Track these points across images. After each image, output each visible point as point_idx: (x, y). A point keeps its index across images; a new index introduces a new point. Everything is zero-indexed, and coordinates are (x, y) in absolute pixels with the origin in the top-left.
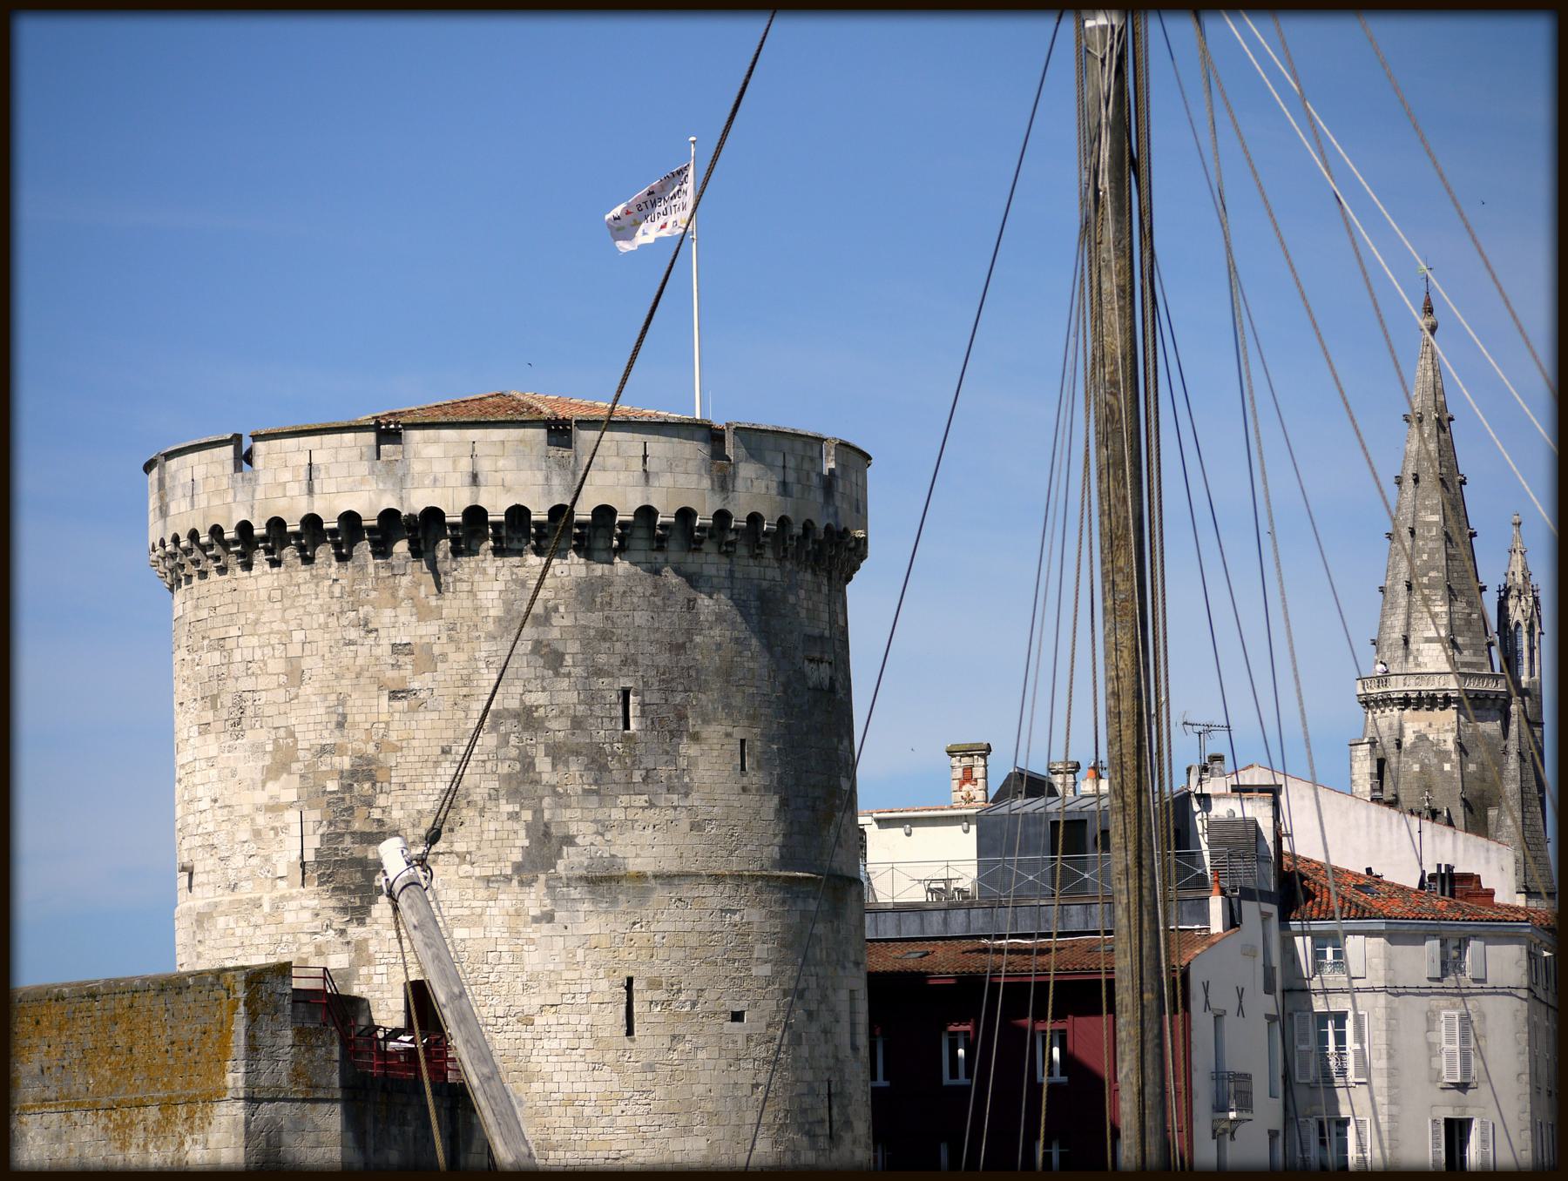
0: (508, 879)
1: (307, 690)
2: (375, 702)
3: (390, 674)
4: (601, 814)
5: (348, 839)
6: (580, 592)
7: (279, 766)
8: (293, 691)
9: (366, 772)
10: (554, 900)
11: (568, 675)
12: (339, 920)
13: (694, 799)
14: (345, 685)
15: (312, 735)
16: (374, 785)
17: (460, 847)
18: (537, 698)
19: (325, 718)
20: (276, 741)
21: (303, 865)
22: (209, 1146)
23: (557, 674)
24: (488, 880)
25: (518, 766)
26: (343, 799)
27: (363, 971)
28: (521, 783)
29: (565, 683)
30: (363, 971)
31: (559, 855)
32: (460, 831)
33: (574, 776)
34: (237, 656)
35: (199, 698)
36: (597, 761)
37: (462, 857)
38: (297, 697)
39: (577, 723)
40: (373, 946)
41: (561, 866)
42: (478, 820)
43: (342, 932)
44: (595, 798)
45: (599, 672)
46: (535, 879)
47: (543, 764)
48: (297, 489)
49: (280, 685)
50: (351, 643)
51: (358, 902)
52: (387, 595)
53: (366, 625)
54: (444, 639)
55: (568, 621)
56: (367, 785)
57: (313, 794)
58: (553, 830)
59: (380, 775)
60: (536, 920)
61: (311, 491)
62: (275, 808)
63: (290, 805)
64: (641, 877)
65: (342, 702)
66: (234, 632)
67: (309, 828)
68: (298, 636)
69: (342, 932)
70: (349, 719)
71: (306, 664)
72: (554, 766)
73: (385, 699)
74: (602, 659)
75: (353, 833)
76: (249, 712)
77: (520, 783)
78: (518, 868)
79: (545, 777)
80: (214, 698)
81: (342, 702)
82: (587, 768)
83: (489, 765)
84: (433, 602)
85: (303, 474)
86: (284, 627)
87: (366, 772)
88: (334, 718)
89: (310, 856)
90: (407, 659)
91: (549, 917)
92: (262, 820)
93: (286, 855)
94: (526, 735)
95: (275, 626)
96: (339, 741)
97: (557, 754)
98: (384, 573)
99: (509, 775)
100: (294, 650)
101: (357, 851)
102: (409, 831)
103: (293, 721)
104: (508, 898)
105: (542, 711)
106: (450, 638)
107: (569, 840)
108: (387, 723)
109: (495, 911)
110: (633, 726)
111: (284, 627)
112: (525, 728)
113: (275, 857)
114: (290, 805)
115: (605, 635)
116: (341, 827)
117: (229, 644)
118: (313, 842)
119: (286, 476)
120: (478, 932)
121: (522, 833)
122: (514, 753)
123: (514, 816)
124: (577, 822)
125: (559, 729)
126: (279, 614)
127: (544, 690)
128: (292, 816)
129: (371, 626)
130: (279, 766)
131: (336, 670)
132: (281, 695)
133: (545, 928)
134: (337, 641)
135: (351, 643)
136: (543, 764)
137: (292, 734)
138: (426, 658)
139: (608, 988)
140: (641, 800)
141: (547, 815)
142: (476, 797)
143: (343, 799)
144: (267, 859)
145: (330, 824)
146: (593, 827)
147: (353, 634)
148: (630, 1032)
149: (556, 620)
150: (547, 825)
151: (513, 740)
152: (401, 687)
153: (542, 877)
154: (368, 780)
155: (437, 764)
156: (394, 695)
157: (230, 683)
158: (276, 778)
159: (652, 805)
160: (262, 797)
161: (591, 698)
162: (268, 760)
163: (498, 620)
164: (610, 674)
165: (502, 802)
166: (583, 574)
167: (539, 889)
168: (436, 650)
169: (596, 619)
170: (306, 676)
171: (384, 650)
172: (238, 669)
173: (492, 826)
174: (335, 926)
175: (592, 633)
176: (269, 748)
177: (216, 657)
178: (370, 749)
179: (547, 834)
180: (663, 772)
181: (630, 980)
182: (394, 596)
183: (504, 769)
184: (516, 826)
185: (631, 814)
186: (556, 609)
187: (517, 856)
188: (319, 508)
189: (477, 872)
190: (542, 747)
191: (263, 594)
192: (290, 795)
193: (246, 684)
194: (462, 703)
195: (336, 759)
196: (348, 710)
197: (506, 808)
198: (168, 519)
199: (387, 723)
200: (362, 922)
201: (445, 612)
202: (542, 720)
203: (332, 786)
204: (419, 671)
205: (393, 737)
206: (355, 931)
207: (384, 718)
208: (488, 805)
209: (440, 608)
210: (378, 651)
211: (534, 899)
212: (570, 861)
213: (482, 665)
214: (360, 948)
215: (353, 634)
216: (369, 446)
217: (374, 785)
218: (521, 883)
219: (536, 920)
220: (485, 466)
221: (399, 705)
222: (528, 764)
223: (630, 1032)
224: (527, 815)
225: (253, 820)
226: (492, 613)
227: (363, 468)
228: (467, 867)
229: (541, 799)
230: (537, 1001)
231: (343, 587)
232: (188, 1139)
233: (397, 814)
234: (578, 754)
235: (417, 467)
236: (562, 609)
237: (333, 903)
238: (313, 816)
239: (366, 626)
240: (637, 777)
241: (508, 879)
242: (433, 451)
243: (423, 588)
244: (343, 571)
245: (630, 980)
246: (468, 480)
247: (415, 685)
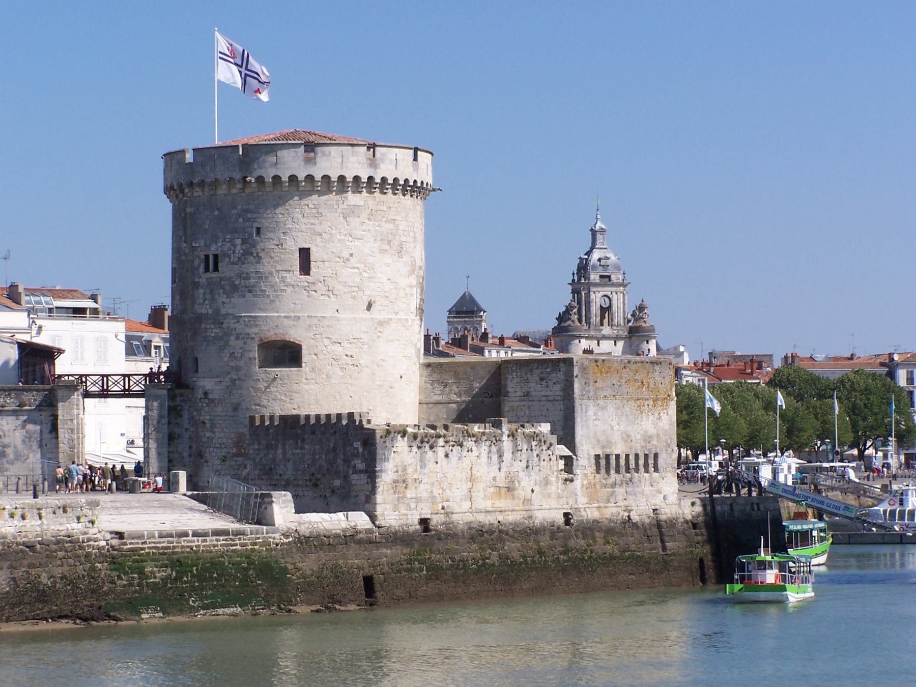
7: (412, 272)
22: (669, 414)
35: (379, 239)
63: (414, 286)
66: (399, 218)
76: (404, 249)
80: (389, 242)
89: (418, 306)
117: (397, 222)
128: (415, 289)
137: (415, 261)
157: (397, 237)
172: (400, 232)
176: (410, 264)
177: (391, 226)
192: (414, 283)
193: (403, 238)
198: (378, 171)
232: (662, 413)
238: (419, 290)
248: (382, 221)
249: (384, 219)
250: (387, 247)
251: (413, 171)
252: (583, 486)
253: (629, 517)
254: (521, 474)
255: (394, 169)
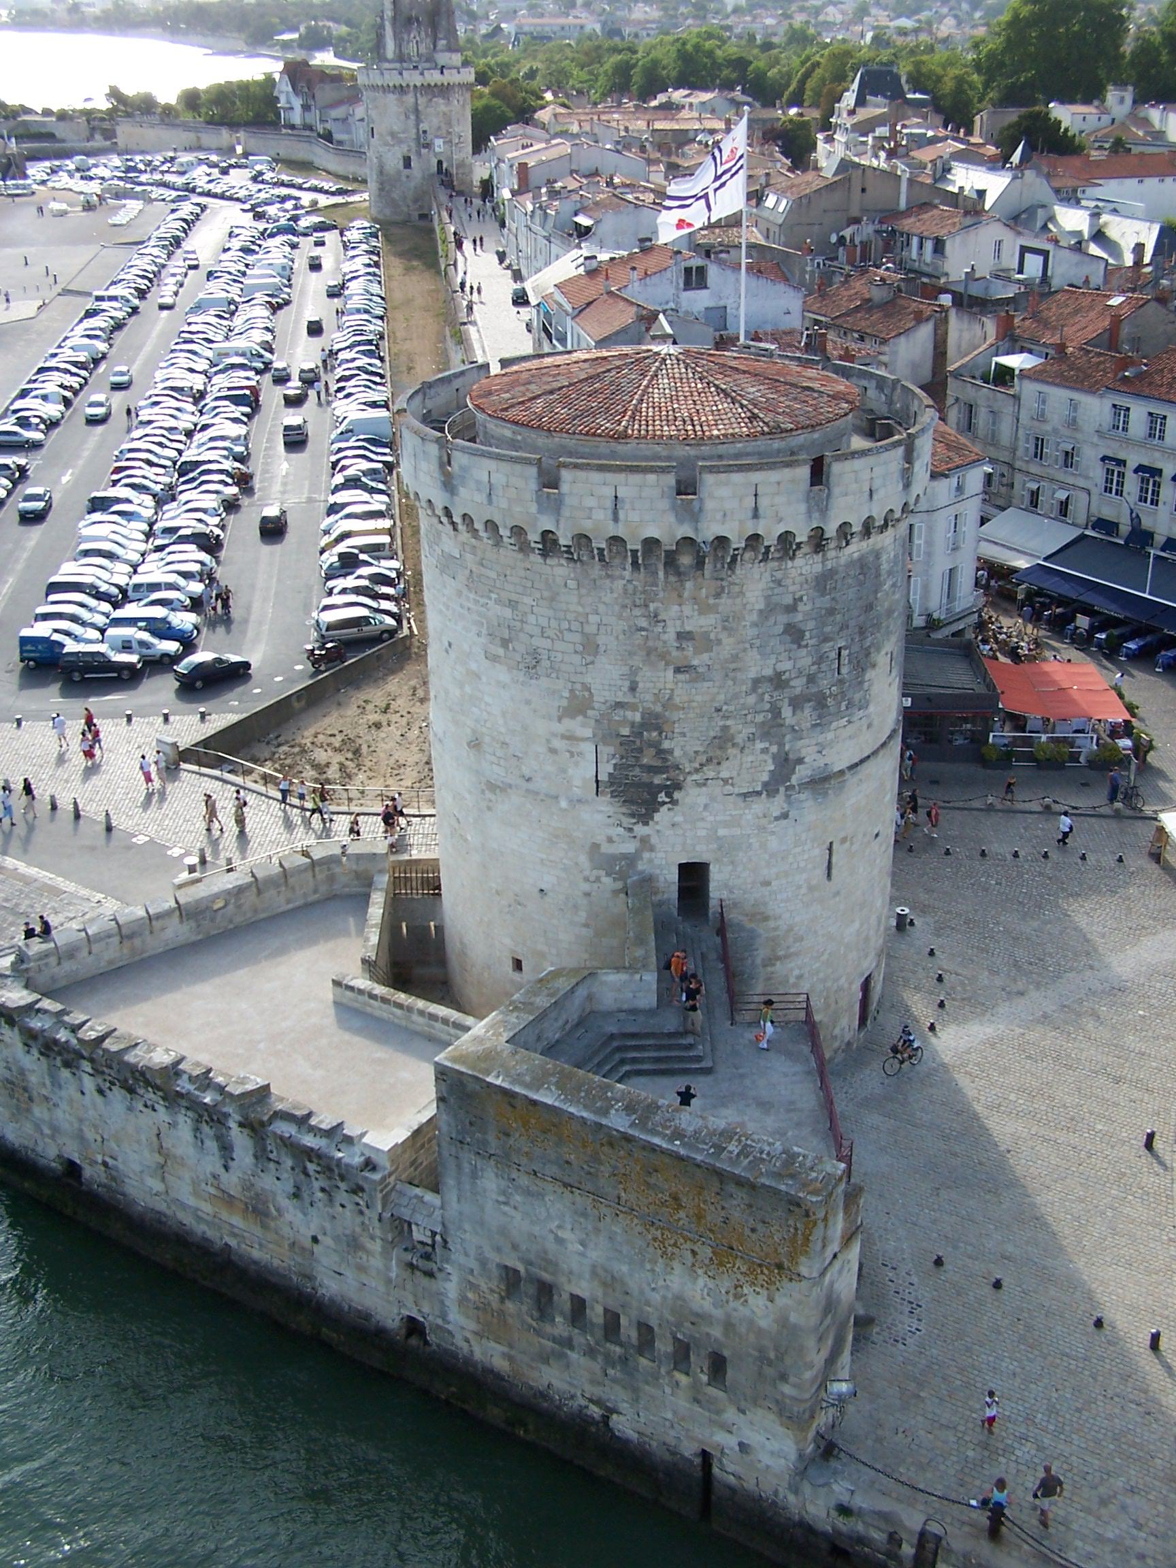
0: (759, 793)
1: (602, 660)
2: (662, 674)
3: (675, 653)
4: (821, 739)
5: (637, 771)
6: (818, 584)
8: (589, 659)
9: (653, 722)
10: (790, 803)
11: (806, 646)
12: (627, 821)
13: (871, 708)
14: (637, 661)
15: (606, 693)
16: (660, 734)
17: (725, 774)
18: (786, 665)
19: (620, 683)
20: (572, 691)
21: (597, 781)
23: (800, 646)
24: (745, 795)
25: (770, 716)
26: (634, 742)
27: (646, 855)
28: (772, 728)
29: (804, 652)
30: (646, 855)
31: (793, 772)
32: (725, 764)
33: (808, 714)
34: (532, 619)
36: (820, 702)
37: (725, 781)
38: (592, 663)
39: (811, 679)
40: (654, 840)
41: (794, 780)
42: (739, 756)
43: (630, 830)
44: (819, 728)
45: (826, 639)
46: (777, 791)
47: (787, 712)
48: (602, 516)
49: (576, 652)
50: (642, 629)
51: (644, 811)
52: (675, 595)
53: (656, 616)
54: (719, 629)
55: (808, 607)
56: (655, 734)
57: (606, 734)
58: (791, 756)
59: (666, 728)
60: (777, 819)
61: (616, 519)
62: (570, 737)
63: (587, 739)
64: (842, 772)
65: (634, 671)
67: (603, 757)
68: (593, 619)
69: (630, 830)
70: (641, 685)
71: (601, 640)
72: (794, 714)
73: (670, 673)
74: (828, 629)
75: (641, 766)
77: (773, 727)
78: (765, 785)
79: (788, 722)
81: (634, 671)
82: (815, 709)
83: (749, 717)
84: (711, 601)
85: (609, 504)
86: (580, 609)
87: (653, 722)
88: (627, 684)
89: (603, 777)
90: (690, 644)
91: (785, 816)
92: (557, 744)
93: (583, 772)
94: (775, 694)
95: (572, 608)
96: (632, 700)
97: (796, 703)
98: (672, 579)
99: (763, 723)
100: (588, 629)
101: (645, 778)
102: (687, 765)
103: (589, 680)
104: (759, 806)
105: (787, 674)
106: (724, 628)
107: (800, 761)
108: (672, 690)
109: (749, 817)
110: (844, 670)
111: (580, 609)
112: (776, 689)
113: (570, 771)
114: (587, 739)
115: (831, 612)
116: (631, 761)
118: (606, 769)
119: (590, 502)
120: (737, 831)
121: (770, 761)
122: (768, 706)
123: (765, 751)
124: (807, 749)
125: (798, 685)
126: (575, 599)
127: (790, 658)
128: (589, 748)
129: (660, 618)
130: (578, 706)
131: (629, 648)
132: (577, 659)
133: (784, 822)
134: (630, 627)
135: (642, 629)
136: (787, 712)
137: (589, 690)
138: (706, 643)
139: (819, 853)
140: (844, 722)
141: (787, 747)
142: (739, 739)
143: (634, 742)
144: (564, 771)
145: (622, 757)
146: (816, 748)
147: (643, 623)
148: (829, 875)
149: (801, 607)
150: (787, 754)
151: (767, 697)
152: (686, 664)
153: (782, 789)
154: (655, 730)
155: (711, 718)
156: (678, 670)
158: (573, 717)
159: (849, 722)
160: (560, 728)
161: (820, 659)
162: (565, 703)
163: (761, 611)
164: (831, 640)
165: (758, 741)
166: (818, 568)
167: (780, 799)
168: (712, 636)
169: (825, 602)
170: (602, 649)
171: (670, 636)
173: (750, 759)
174: (625, 825)
175: (823, 612)
176: (567, 694)
177: (508, 613)
178: (659, 709)
179: (786, 760)
180: (857, 696)
181: (831, 843)
182: (680, 596)
183: (760, 718)
184: (765, 757)
185: (838, 731)
186: (801, 599)
187: (765, 777)
188: (621, 531)
189: (737, 790)
190: (786, 701)
191: (559, 581)
192: (588, 733)
194: (731, 675)
195: (629, 714)
196: (638, 679)
197: (760, 745)
199: (672, 690)
200: (646, 824)
201: (720, 609)
202: (788, 681)
203: (625, 731)
204: (697, 652)
205: (677, 700)
206: (640, 830)
207: (669, 686)
208: (748, 744)
209: (716, 605)
210: (665, 637)
211: (777, 805)
212: (801, 773)
213: (747, 646)
214: (645, 841)
215: (643, 623)
216: (670, 488)
217: (660, 734)
218: (768, 795)
219: (777, 819)
220: (764, 502)
221: (681, 677)
222: (776, 712)
223: (829, 875)
224: (774, 749)
225: (548, 741)
226: (757, 607)
227: (664, 504)
228: (728, 788)
229: (784, 736)
230: (774, 870)
231: (635, 587)
233: (677, 753)
234: (809, 701)
235: (709, 505)
236: (805, 598)
237: (624, 810)
238: (611, 750)
239: (655, 618)
240: (843, 708)
241: (759, 793)
242: (723, 492)
243: (704, 590)
244: (636, 575)
245: (831, 843)
246: (750, 514)
247: (695, 662)
248: (490, 599)
249: (494, 596)
250: (501, 651)
251: (540, 511)
252: (463, 1300)
253: (606, 1419)
254: (284, 1202)
255: (485, 502)
